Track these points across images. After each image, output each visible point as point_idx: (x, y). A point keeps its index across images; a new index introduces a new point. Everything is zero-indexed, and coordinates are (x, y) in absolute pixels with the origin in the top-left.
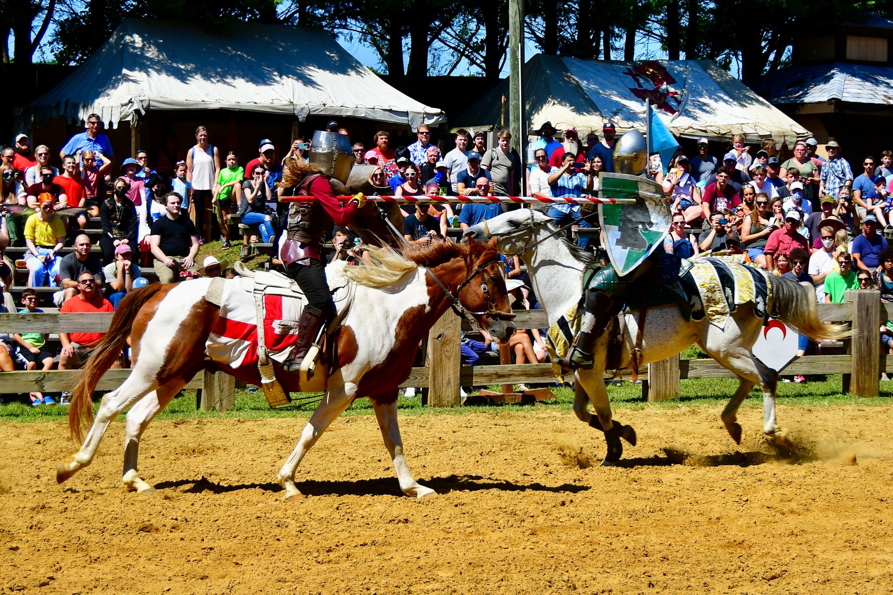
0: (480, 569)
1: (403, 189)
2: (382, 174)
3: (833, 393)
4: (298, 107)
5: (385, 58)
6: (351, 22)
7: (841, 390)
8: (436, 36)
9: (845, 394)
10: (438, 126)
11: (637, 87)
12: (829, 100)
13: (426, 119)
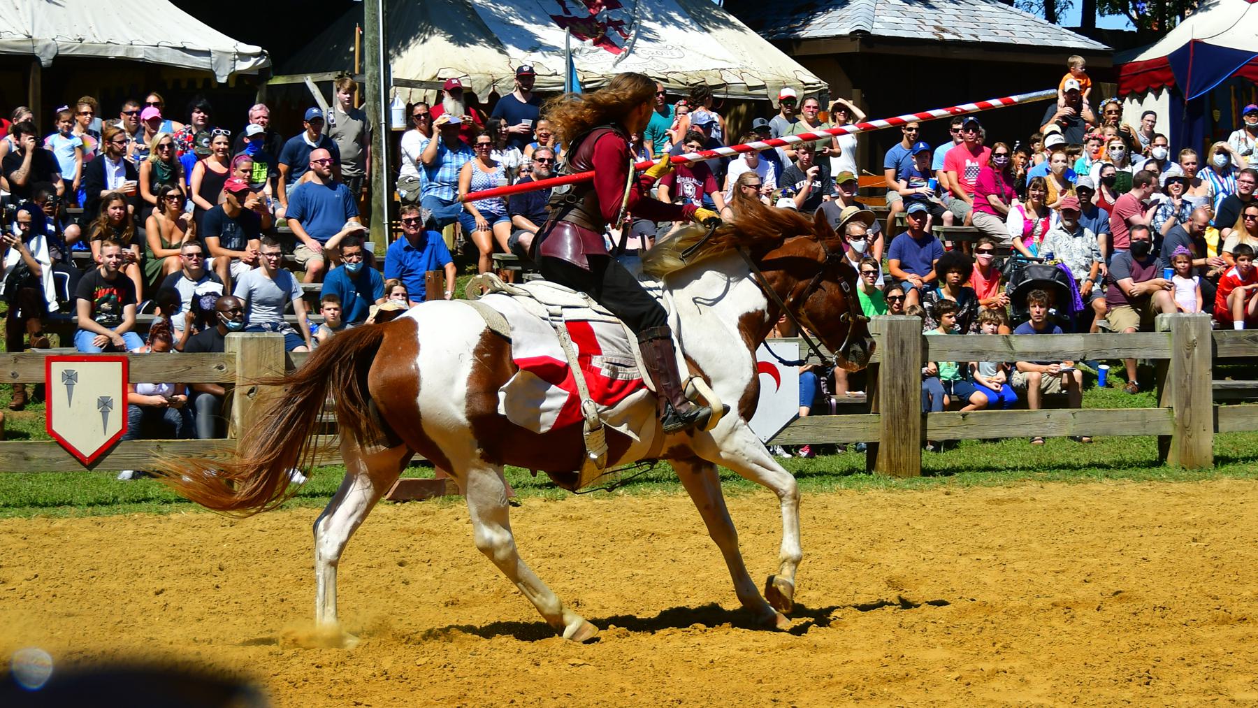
1: (206, 167)
2: (171, 145)
3: (851, 472)
4: (40, 45)
7: (864, 467)
9: (871, 474)
10: (256, 73)
11: (562, 13)
12: (852, 33)
13: (238, 62)
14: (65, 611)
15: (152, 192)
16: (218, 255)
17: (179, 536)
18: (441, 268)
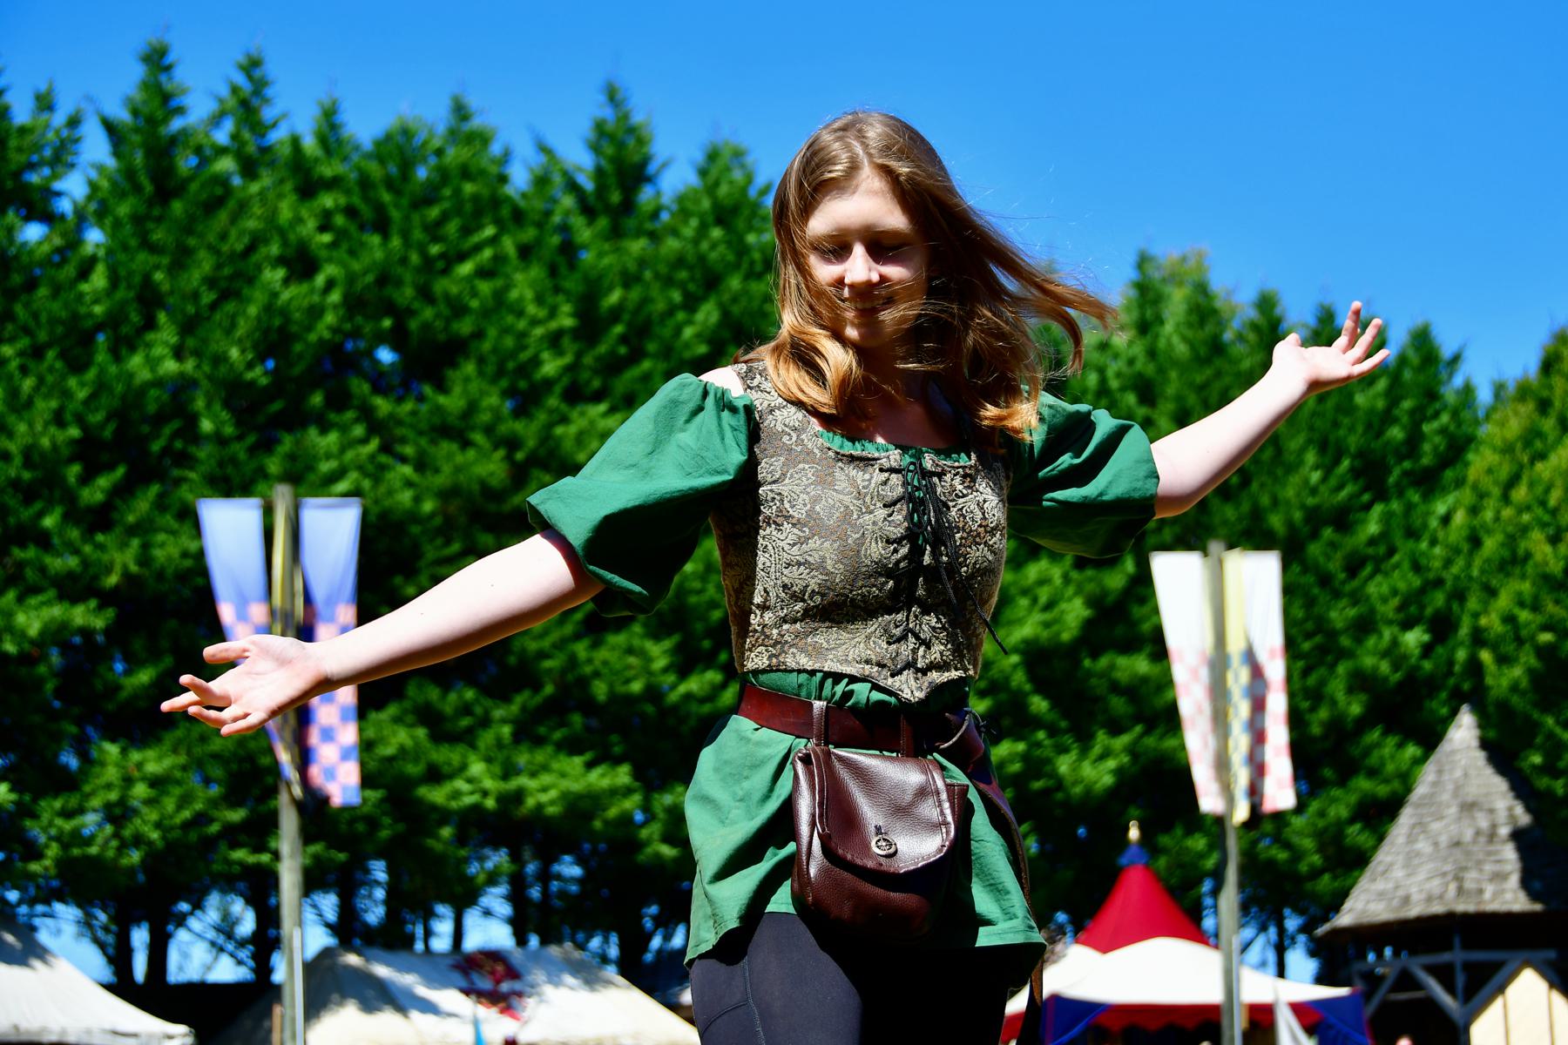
5: (111, 960)
6: (59, 907)
8: (181, 921)
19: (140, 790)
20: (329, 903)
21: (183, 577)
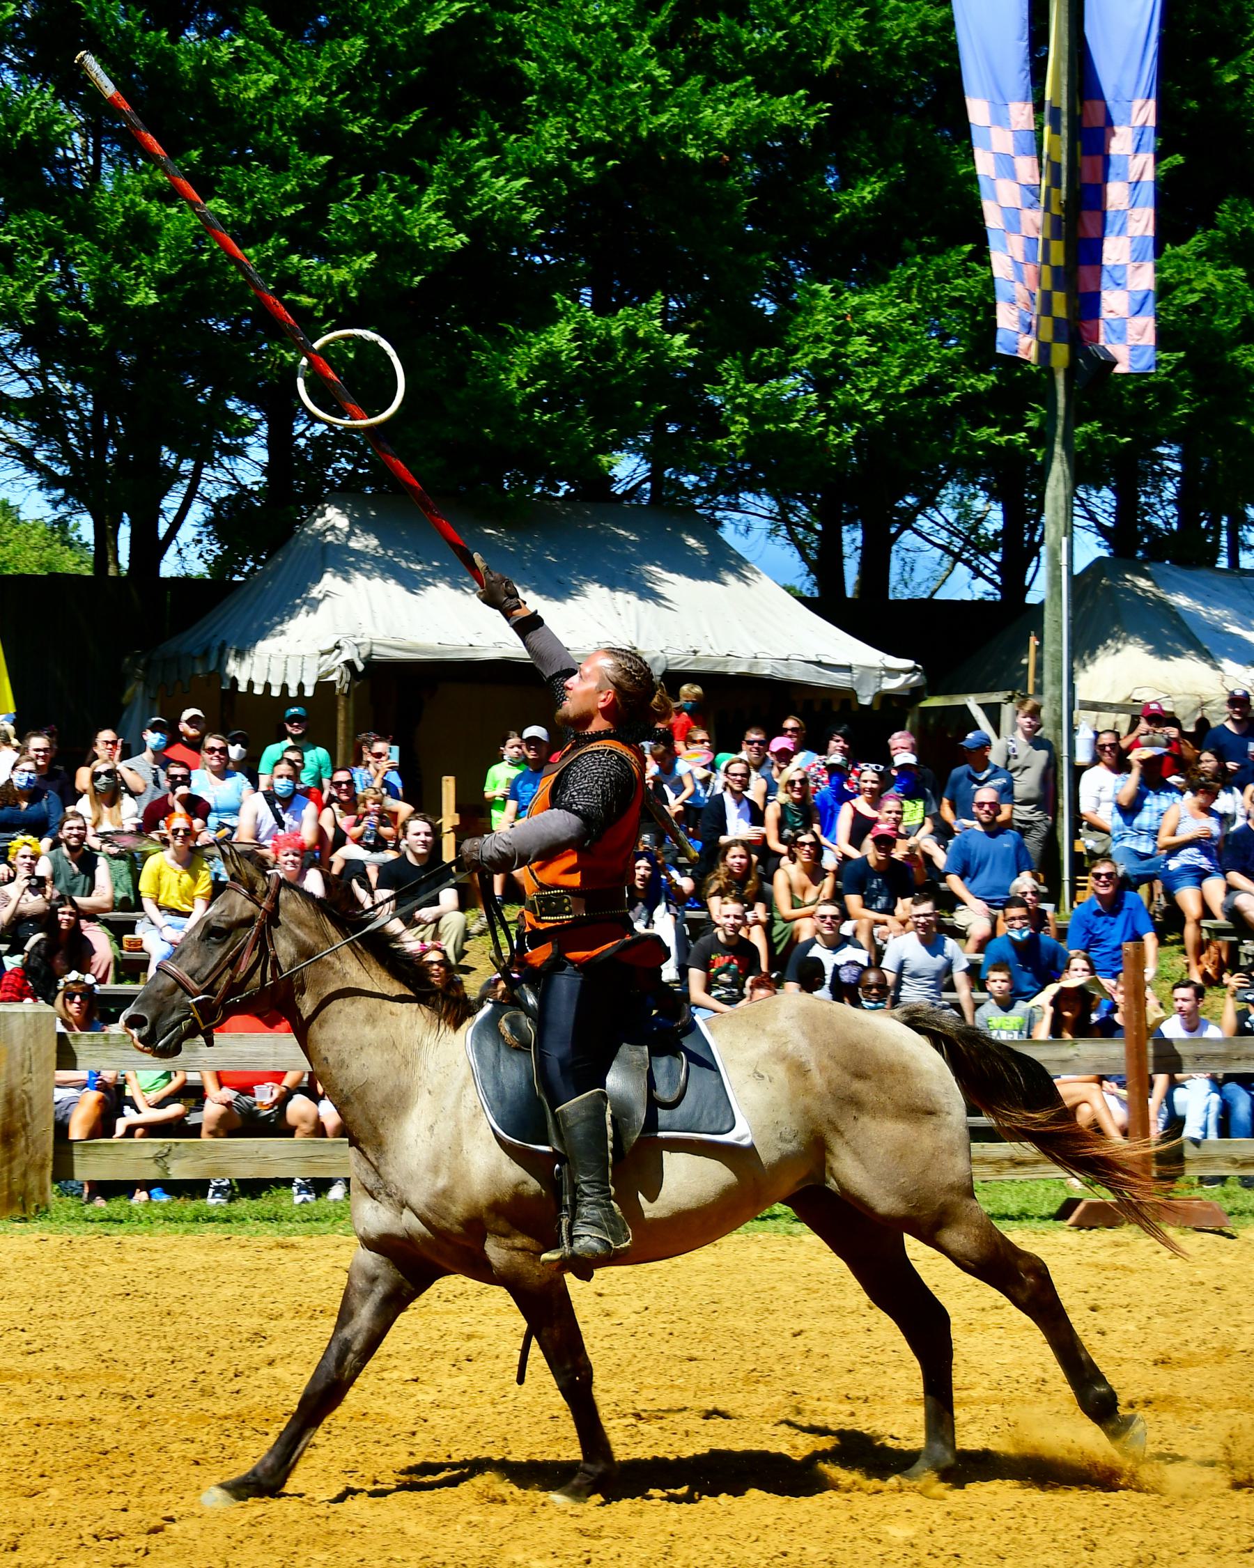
0: (968, 1524)
2: (804, 781)
5: (813, 568)
6: (746, 498)
14: (686, 1354)
15: (781, 840)
16: (859, 918)
17: (814, 1263)
18: (1137, 938)
19: (859, 346)
20: (1104, 501)
21: (921, 58)
